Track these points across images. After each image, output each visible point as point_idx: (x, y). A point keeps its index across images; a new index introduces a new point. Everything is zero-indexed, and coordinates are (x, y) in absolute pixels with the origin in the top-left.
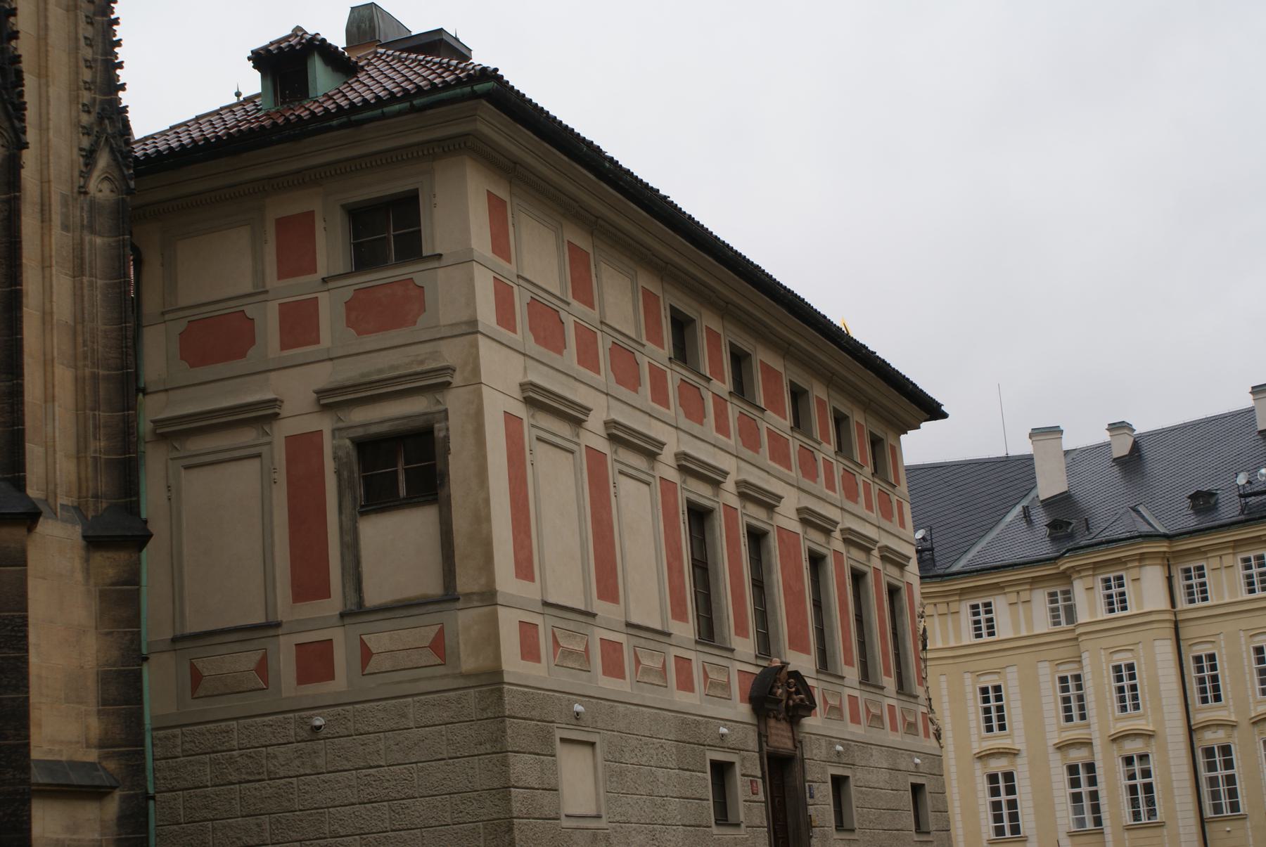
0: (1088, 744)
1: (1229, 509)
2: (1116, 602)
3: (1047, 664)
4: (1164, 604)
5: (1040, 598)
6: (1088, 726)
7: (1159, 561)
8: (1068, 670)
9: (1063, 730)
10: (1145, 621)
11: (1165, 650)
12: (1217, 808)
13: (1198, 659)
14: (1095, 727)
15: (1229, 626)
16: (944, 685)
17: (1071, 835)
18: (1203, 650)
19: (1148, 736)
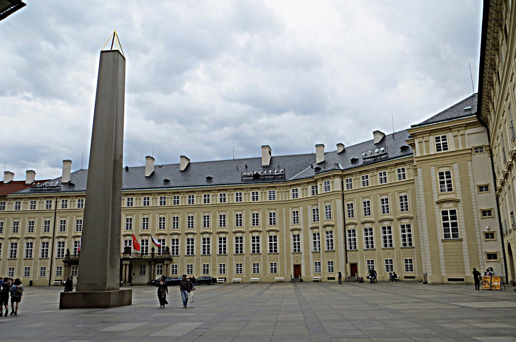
0: (318, 228)
1: (361, 162)
2: (327, 188)
3: (310, 206)
4: (340, 189)
5: (310, 187)
6: (318, 223)
7: (339, 177)
8: (315, 208)
9: (312, 224)
10: (335, 193)
11: (340, 202)
12: (351, 248)
13: (348, 205)
14: (320, 223)
15: (357, 196)
16: (284, 210)
17: (313, 253)
18: (350, 202)
19: (333, 226)
